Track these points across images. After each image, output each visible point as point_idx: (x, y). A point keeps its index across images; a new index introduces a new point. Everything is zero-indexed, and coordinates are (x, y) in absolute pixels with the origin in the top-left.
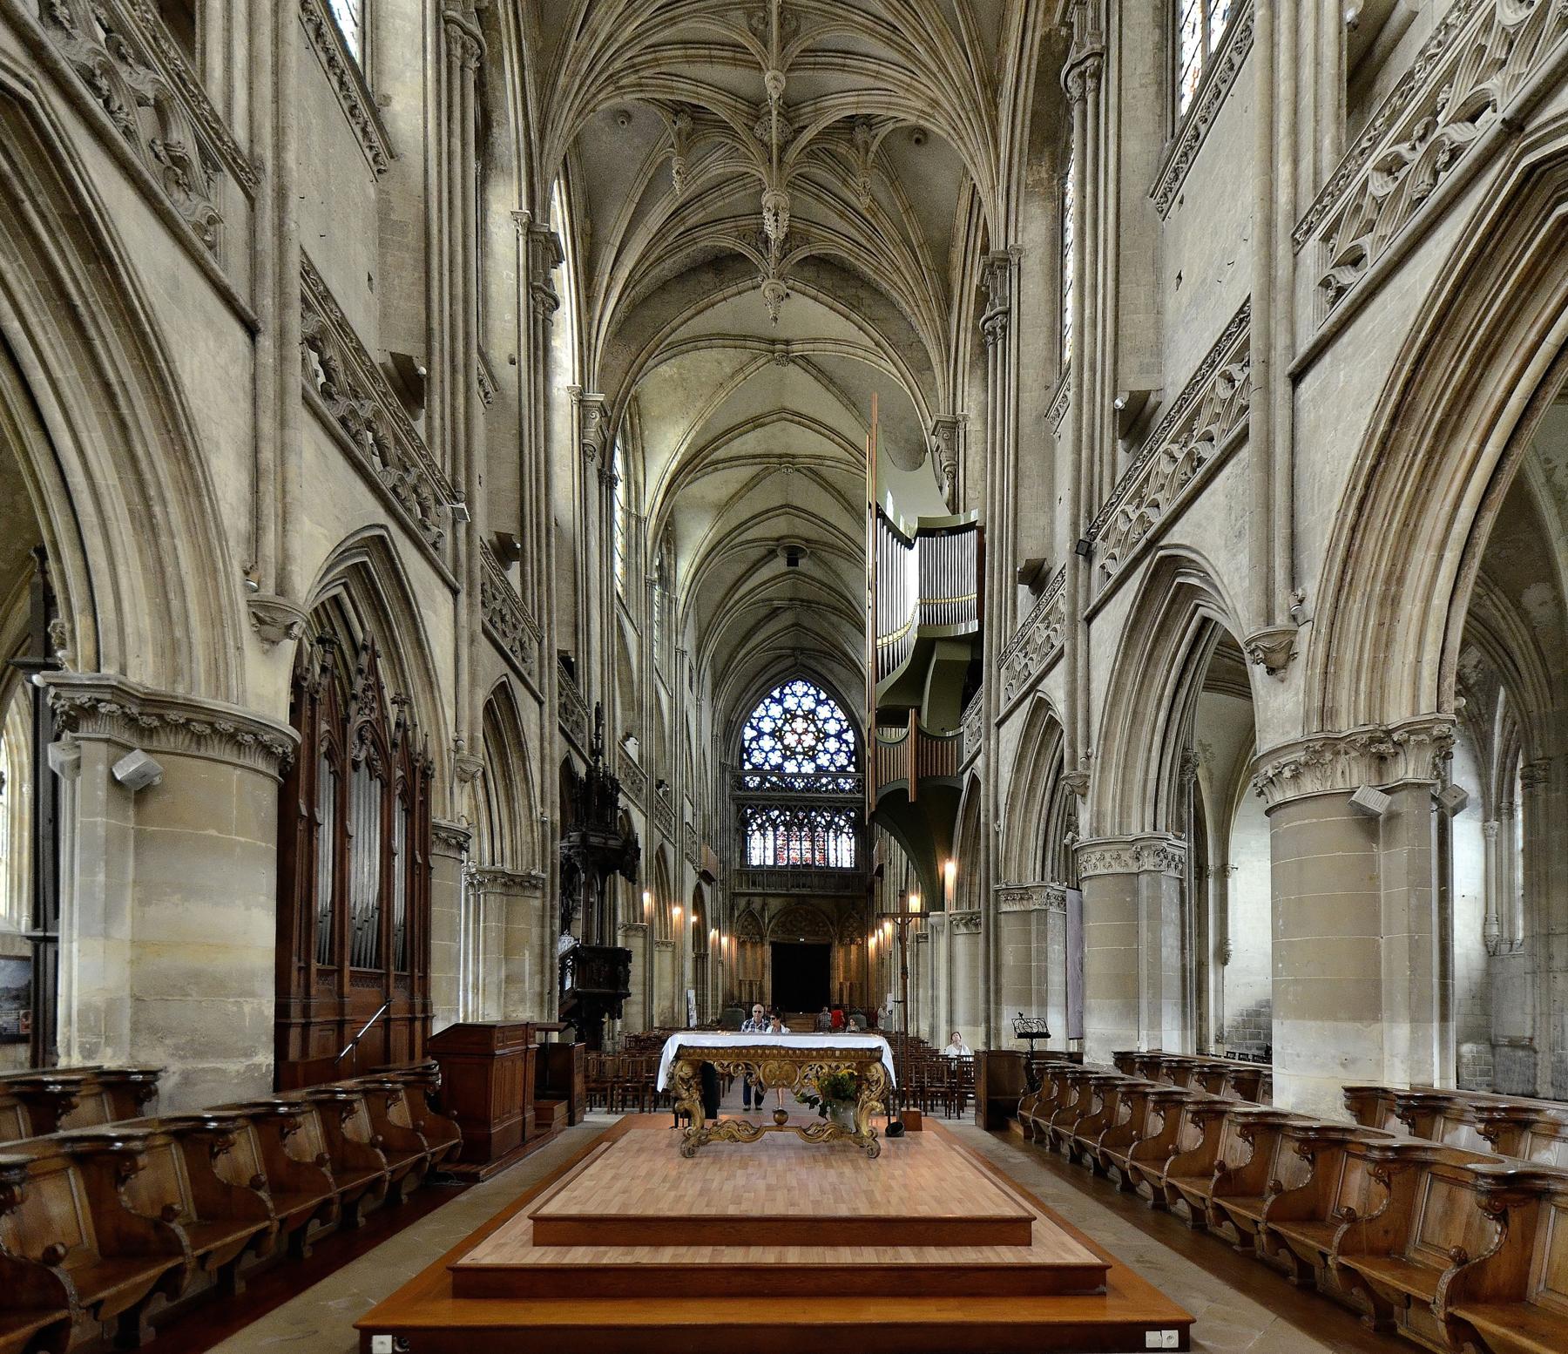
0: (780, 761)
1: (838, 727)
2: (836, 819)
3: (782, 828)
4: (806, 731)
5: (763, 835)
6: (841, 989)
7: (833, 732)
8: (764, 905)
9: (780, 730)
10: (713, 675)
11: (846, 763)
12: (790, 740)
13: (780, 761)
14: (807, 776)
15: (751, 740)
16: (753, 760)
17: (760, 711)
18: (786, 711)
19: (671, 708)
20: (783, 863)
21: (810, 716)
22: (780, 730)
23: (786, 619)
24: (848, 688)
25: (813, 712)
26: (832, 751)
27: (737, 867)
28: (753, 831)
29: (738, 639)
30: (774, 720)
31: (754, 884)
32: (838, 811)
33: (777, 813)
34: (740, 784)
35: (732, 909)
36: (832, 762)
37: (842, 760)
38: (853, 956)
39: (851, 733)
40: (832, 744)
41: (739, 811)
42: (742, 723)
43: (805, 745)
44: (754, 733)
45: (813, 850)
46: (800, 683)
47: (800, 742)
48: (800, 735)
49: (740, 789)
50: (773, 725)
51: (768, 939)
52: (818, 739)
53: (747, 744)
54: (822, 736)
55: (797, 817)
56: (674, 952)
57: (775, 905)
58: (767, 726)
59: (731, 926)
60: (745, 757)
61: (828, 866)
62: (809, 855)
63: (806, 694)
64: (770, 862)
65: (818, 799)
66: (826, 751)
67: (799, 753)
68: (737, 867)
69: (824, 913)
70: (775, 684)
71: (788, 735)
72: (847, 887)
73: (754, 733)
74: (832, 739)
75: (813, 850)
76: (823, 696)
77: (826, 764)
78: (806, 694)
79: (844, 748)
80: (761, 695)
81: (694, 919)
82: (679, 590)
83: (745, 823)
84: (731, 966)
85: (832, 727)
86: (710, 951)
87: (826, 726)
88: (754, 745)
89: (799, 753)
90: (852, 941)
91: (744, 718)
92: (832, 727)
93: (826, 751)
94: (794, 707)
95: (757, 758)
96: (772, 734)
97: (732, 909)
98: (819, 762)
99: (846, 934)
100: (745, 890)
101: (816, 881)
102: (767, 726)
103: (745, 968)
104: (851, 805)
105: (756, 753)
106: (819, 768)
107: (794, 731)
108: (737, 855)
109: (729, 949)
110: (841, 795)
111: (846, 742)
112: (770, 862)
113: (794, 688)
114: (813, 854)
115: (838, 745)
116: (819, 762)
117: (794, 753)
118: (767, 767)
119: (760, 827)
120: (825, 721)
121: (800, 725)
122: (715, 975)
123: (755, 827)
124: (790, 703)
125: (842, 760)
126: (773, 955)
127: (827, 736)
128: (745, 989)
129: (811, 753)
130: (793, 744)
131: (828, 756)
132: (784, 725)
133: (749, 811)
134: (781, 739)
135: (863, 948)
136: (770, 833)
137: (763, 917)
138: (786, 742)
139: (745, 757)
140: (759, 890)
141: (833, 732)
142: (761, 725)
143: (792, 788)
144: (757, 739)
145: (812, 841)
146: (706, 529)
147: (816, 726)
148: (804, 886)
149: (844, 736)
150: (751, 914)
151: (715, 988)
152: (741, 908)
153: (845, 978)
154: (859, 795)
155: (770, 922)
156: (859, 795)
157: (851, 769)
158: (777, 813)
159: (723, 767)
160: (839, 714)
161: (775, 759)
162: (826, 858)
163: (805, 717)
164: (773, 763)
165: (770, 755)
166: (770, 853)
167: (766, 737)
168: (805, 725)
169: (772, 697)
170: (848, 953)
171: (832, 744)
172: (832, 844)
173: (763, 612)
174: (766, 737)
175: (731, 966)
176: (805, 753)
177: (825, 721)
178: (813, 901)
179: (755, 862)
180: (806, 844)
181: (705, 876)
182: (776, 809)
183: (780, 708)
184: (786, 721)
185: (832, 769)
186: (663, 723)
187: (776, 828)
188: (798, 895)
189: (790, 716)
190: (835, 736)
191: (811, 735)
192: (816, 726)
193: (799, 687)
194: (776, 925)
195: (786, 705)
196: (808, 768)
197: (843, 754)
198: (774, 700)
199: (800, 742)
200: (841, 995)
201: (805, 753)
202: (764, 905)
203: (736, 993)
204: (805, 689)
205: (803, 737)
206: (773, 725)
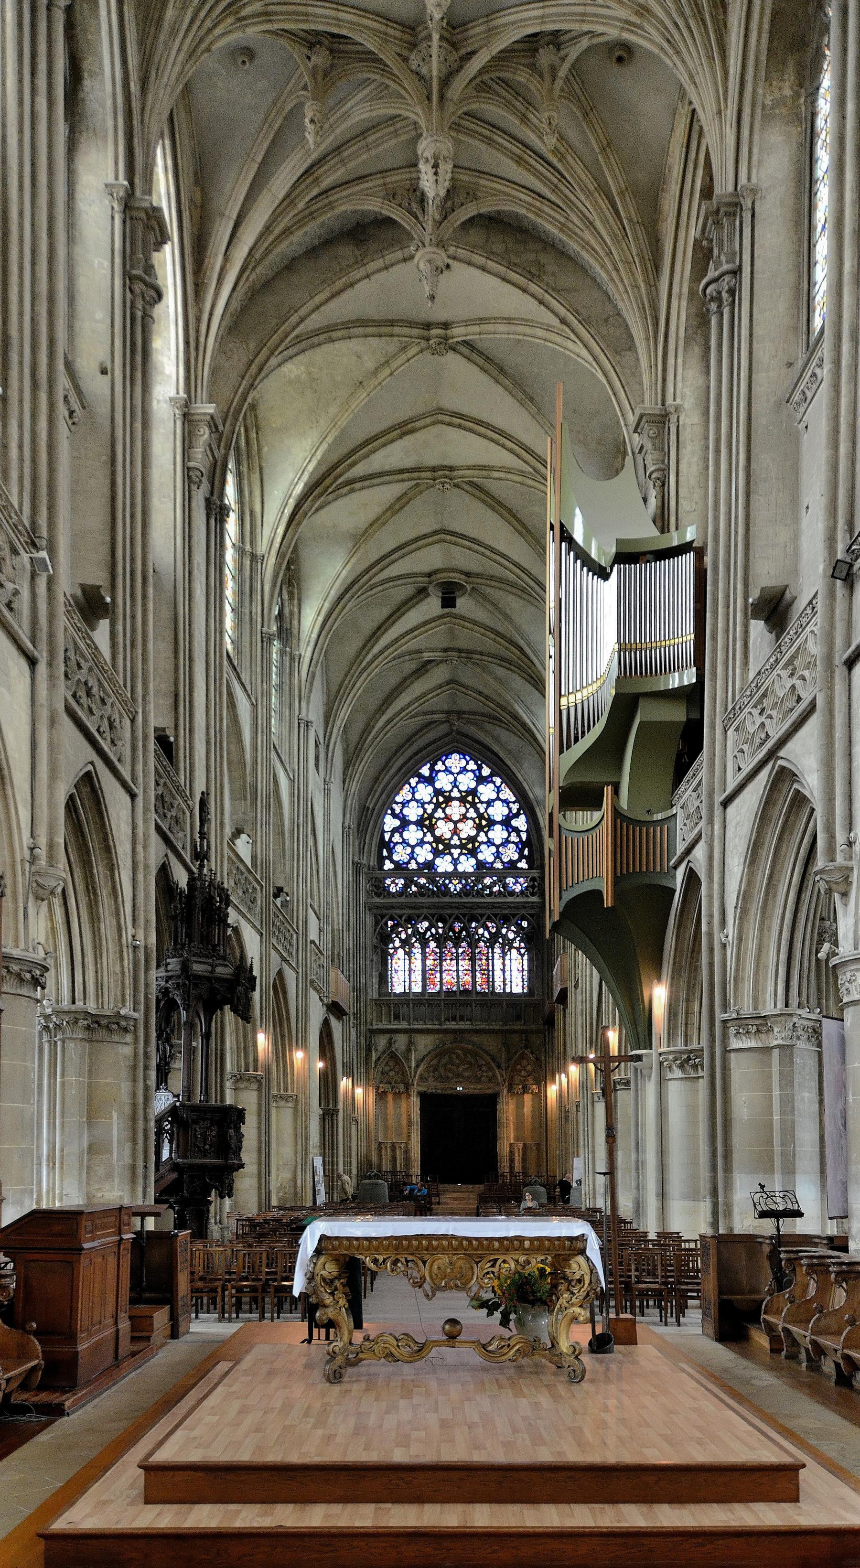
0: (430, 857)
1: (506, 811)
2: (504, 931)
3: (433, 944)
4: (464, 818)
5: (409, 954)
6: (512, 1153)
7: (498, 818)
8: (410, 1043)
9: (431, 816)
10: (345, 751)
11: (516, 857)
12: (444, 829)
13: (430, 857)
14: (464, 875)
15: (393, 831)
16: (396, 857)
17: (404, 794)
18: (438, 792)
19: (292, 795)
20: (433, 989)
21: (469, 797)
22: (431, 816)
23: (439, 675)
24: (518, 760)
25: (473, 792)
26: (498, 842)
27: (375, 996)
28: (395, 949)
29: (378, 702)
30: (423, 804)
31: (397, 1017)
32: (506, 920)
33: (426, 924)
34: (379, 889)
35: (369, 1049)
36: (498, 855)
37: (510, 853)
38: (527, 1109)
39: (523, 818)
40: (498, 834)
41: (377, 923)
42: (381, 810)
43: (463, 835)
44: (397, 823)
45: (473, 971)
46: (456, 756)
47: (455, 832)
48: (455, 823)
49: (378, 895)
50: (420, 811)
51: (415, 1089)
52: (479, 828)
53: (387, 837)
54: (485, 823)
55: (452, 929)
56: (295, 1108)
57: (424, 1044)
58: (413, 812)
59: (367, 1072)
60: (385, 853)
61: (493, 992)
62: (468, 978)
63: (464, 770)
64: (417, 988)
65: (479, 905)
66: (490, 843)
67: (456, 847)
68: (375, 996)
69: (487, 1052)
70: (423, 759)
71: (440, 823)
72: (518, 1018)
73: (397, 823)
74: (498, 827)
75: (473, 971)
76: (486, 771)
77: (490, 859)
78: (464, 770)
79: (514, 838)
80: (405, 775)
81: (320, 1065)
82: (303, 645)
83: (385, 939)
84: (367, 1126)
85: (498, 812)
86: (340, 1106)
87: (491, 811)
89: (456, 847)
90: (525, 1090)
91: (384, 804)
92: (498, 812)
93: (490, 843)
94: (448, 787)
95: (401, 854)
96: (420, 823)
97: (369, 1049)
98: (481, 857)
99: (517, 1079)
100: (384, 1025)
101: (477, 1011)
102: (413, 812)
103: (386, 1128)
104: (523, 912)
105: (399, 848)
106: (480, 865)
107: (448, 818)
108: (375, 980)
109: (365, 1101)
110: (510, 899)
111: (517, 831)
112: (417, 988)
113: (448, 763)
114: (474, 977)
115: (505, 834)
116: (481, 857)
117: (448, 847)
118: (413, 865)
119: (405, 943)
120: (489, 803)
121: (455, 810)
122: (347, 1136)
123: (397, 943)
124: (443, 782)
125: (510, 853)
126: (422, 1109)
127: (491, 823)
128: (386, 1154)
129: (470, 847)
130: (448, 835)
131: (493, 849)
132: (435, 810)
133: (390, 923)
134: (431, 829)
135: (540, 1097)
136: (417, 951)
137: (408, 1059)
138: (438, 833)
139: (385, 853)
140: (403, 1025)
141: (498, 818)
142: (406, 811)
143: (446, 892)
144: (400, 829)
145: (473, 960)
146: (339, 567)
147: (477, 810)
148: (462, 1018)
149: (514, 823)
150: (394, 1056)
151: (348, 1155)
152: (380, 1049)
153: (517, 1139)
154: (534, 899)
155: (417, 1066)
156: (534, 899)
157: (523, 865)
158: (426, 924)
159: (357, 868)
160: (507, 794)
161: (424, 854)
162: (490, 982)
163: (462, 800)
164: (421, 860)
165: (418, 850)
166: (417, 977)
167: (412, 827)
168: (463, 810)
169: (420, 776)
170: (520, 1106)
171: (498, 834)
172: (498, 964)
173: (410, 666)
174: (412, 827)
175: (367, 1126)
176: (462, 846)
177: (489, 803)
178: (475, 1038)
179: (398, 989)
180: (465, 964)
181: (335, 1009)
182: (426, 919)
183: (430, 789)
184: (438, 805)
185: (498, 865)
186: (281, 814)
187: (424, 944)
188: (454, 1032)
189: (443, 798)
190: (501, 823)
191: (470, 823)
192: (477, 810)
193: (455, 761)
194: (427, 1070)
195: (438, 785)
196: (467, 865)
197: (511, 846)
198: (423, 779)
199: (455, 832)
200: (512, 1160)
201: (462, 846)
202: (410, 1043)
203: (375, 1159)
204: (463, 763)
205: (460, 826)
206: (420, 811)
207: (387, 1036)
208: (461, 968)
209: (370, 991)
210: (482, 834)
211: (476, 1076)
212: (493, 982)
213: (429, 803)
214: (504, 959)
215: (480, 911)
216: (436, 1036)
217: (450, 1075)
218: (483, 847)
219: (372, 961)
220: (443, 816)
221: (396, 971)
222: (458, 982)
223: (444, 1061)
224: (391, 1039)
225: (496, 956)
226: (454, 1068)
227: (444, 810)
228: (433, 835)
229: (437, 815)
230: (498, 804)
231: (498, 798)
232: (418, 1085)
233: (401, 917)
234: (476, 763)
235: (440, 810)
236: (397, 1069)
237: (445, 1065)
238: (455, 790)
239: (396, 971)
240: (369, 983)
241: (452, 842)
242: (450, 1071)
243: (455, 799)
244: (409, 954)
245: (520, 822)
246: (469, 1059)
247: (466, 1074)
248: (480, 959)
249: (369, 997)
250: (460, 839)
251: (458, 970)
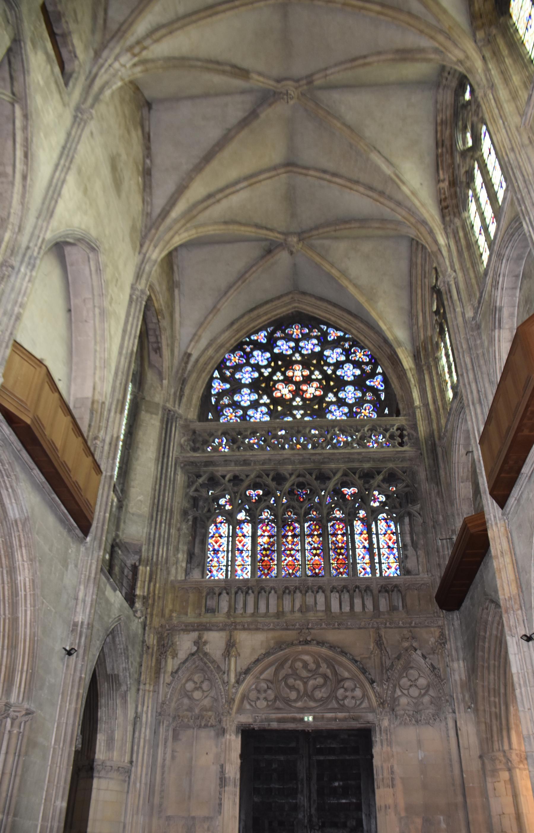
4: (307, 380)
47: (297, 392)
49: (194, 450)
52: (327, 389)
53: (213, 400)
66: (341, 403)
67: (297, 408)
74: (350, 388)
79: (369, 396)
88: (226, 400)
89: (297, 408)
93: (341, 403)
96: (254, 386)
100: (191, 618)
105: (228, 412)
111: (374, 390)
127: (341, 383)
134: (269, 391)
145: (324, 535)
155: (238, 682)
163: (306, 363)
167: (246, 391)
172: (360, 540)
174: (246, 391)
192: (323, 372)
198: (257, 345)
207: (194, 635)
208: (307, 547)
209: (173, 571)
210: (330, 395)
212: (355, 563)
213: (266, 367)
214: (370, 532)
215: (333, 466)
218: (333, 408)
219: (179, 530)
220: (281, 378)
221: (216, 552)
222: (304, 565)
224: (200, 637)
225: (358, 526)
226: (299, 684)
227: (283, 373)
228: (270, 396)
229: (275, 378)
230: (348, 367)
231: (348, 361)
233: (224, 477)
234: (320, 330)
235: (279, 374)
236: (205, 686)
238: (297, 355)
239: (216, 552)
240: (172, 559)
241: (294, 404)
242: (292, 688)
243: (297, 362)
244: (236, 524)
245: (377, 382)
247: (319, 694)
248: (335, 535)
249: (172, 578)
250: (304, 399)
251: (303, 550)
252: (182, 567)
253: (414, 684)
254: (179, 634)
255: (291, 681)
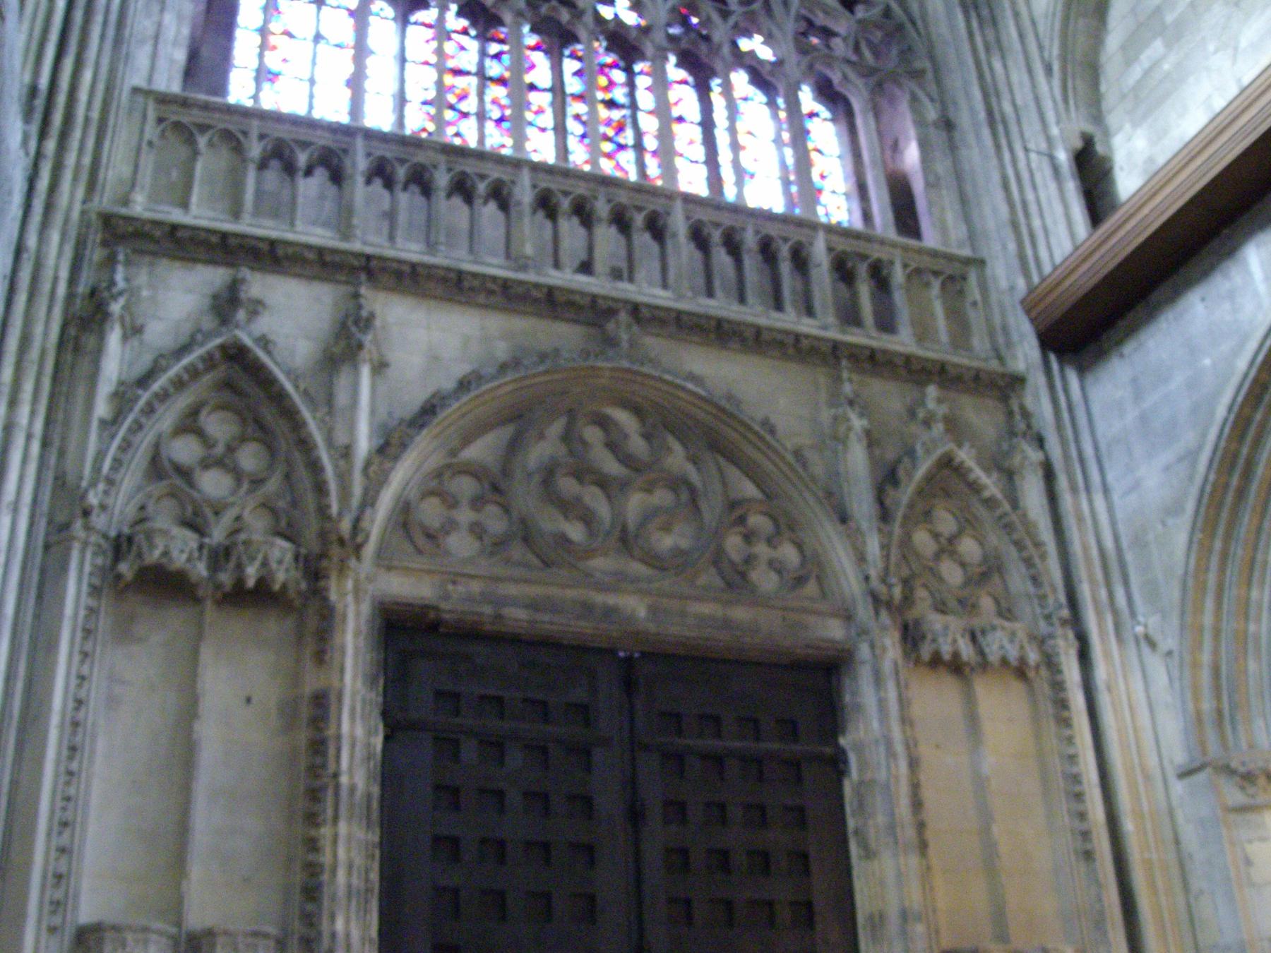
27: (169, 81)
68: (169, 81)
207: (213, 277)
209: (142, 58)
211: (718, 558)
216: (496, 323)
217: (575, 532)
223: (540, 452)
224: (234, 287)
232: (385, 560)
237: (549, 474)
242: (567, 507)
246: (677, 459)
252: (172, 61)
253: (948, 547)
254: (151, 264)
255: (567, 485)
